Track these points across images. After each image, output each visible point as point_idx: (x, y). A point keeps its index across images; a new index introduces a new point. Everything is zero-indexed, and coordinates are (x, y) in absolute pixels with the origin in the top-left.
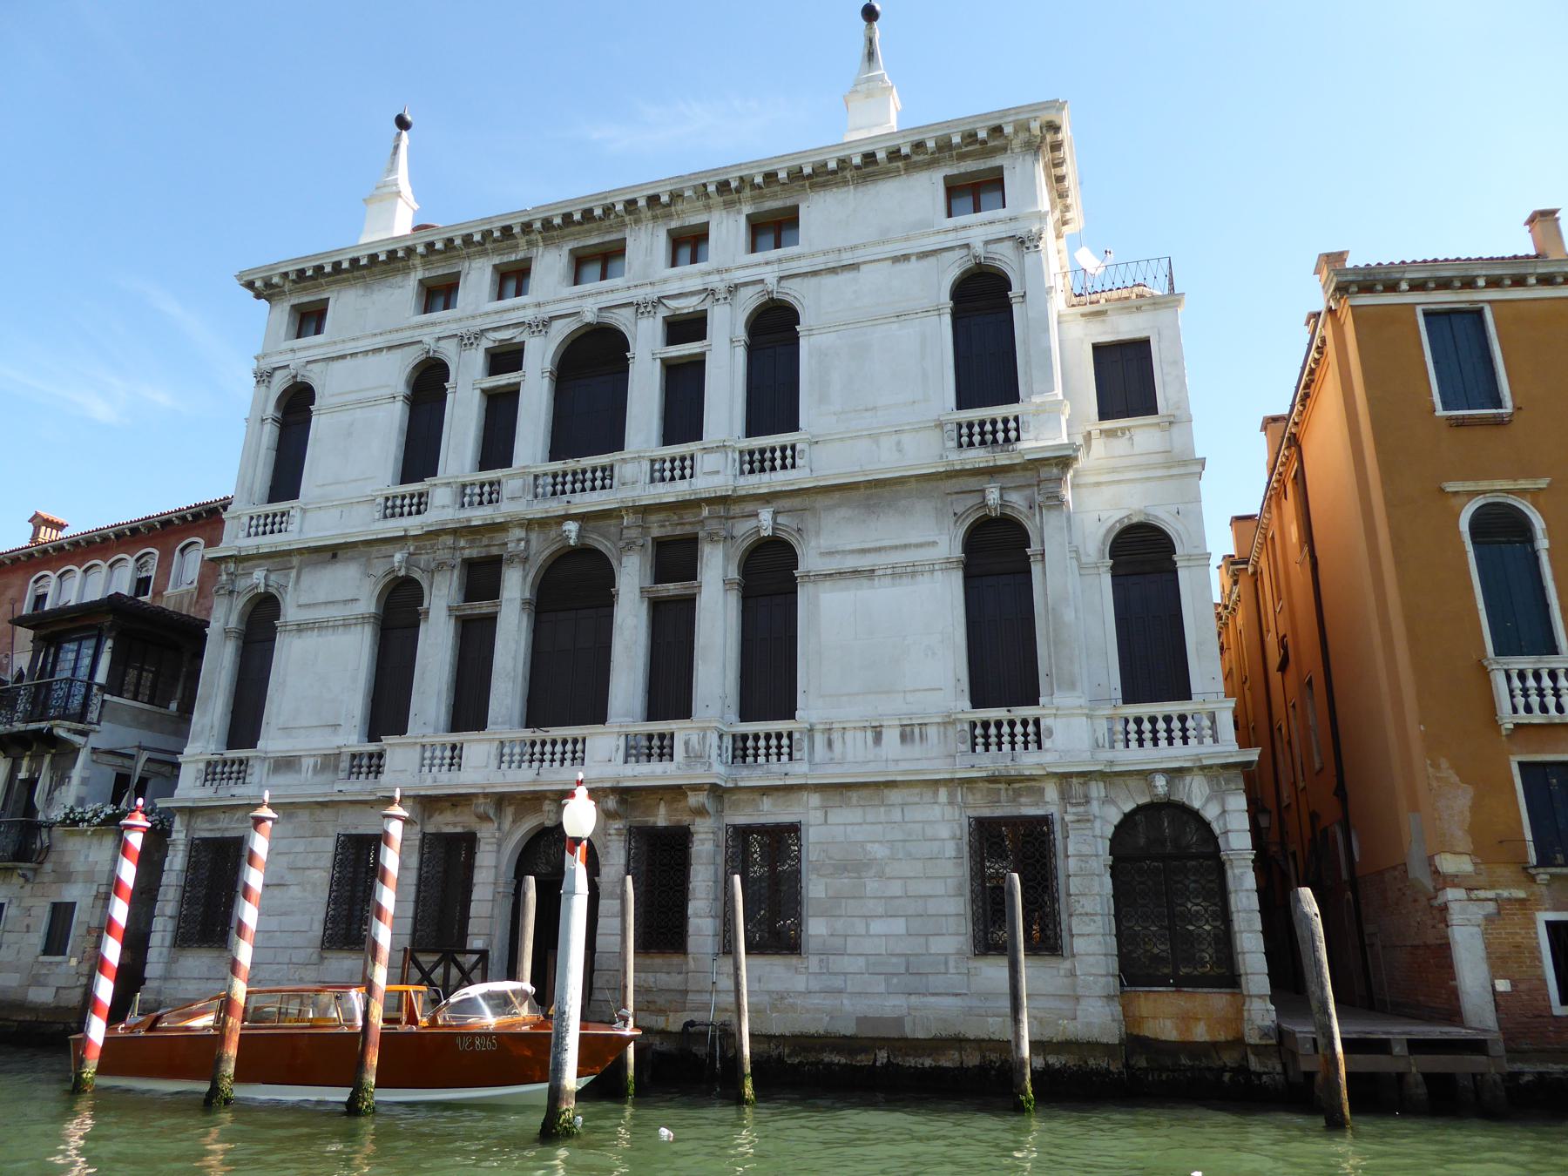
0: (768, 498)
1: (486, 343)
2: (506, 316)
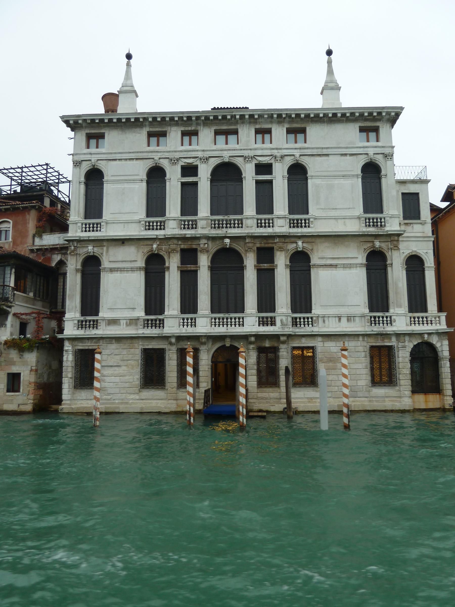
0: (300, 237)
1: (181, 163)
2: (190, 153)
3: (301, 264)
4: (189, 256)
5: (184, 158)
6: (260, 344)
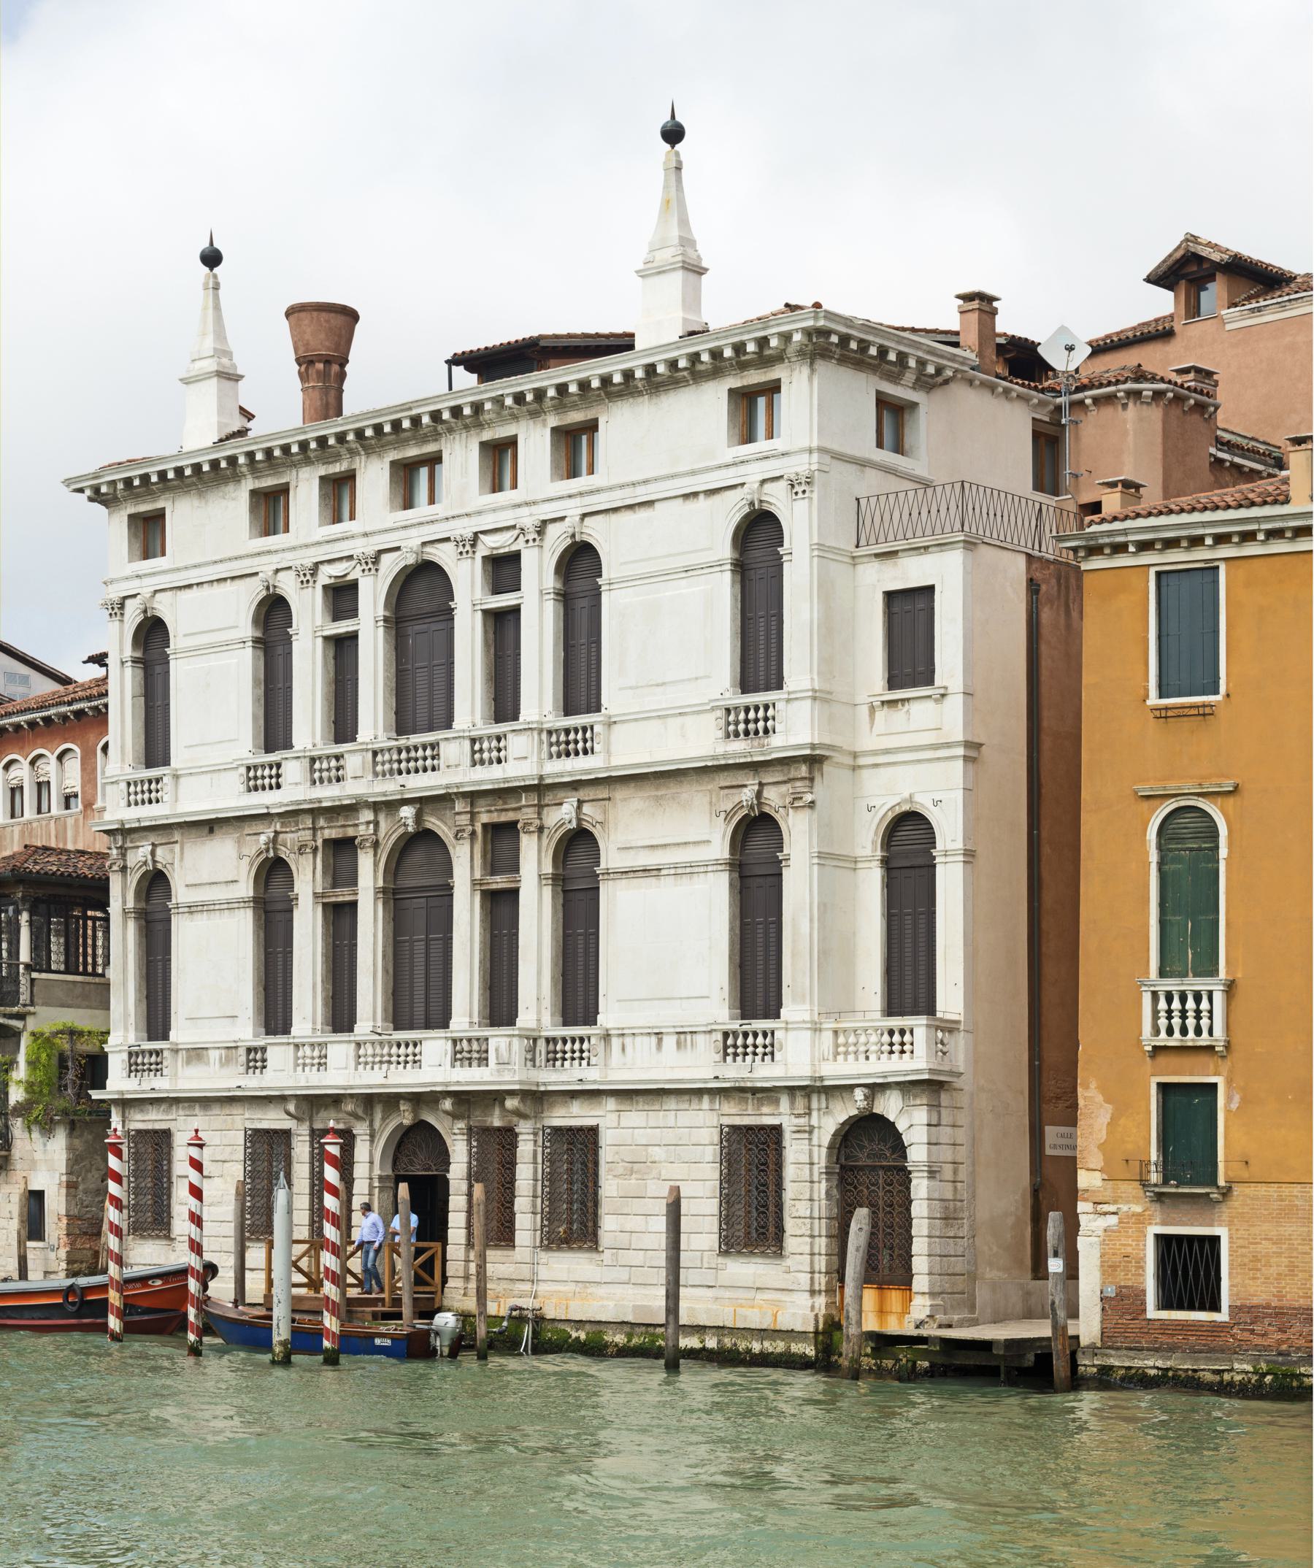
0: (575, 785)
5: (330, 561)
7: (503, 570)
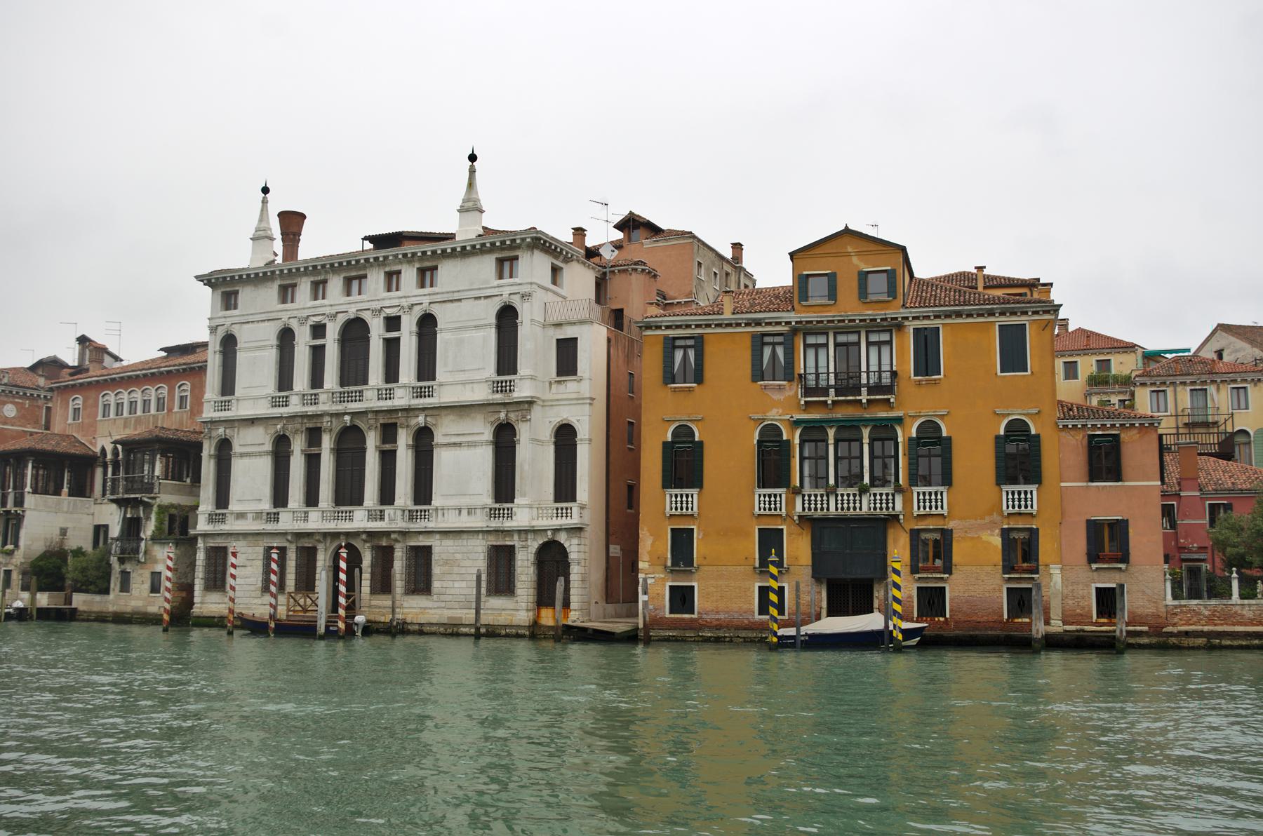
0: (424, 409)
3: (424, 443)
4: (314, 436)
6: (376, 542)
7: (393, 323)
